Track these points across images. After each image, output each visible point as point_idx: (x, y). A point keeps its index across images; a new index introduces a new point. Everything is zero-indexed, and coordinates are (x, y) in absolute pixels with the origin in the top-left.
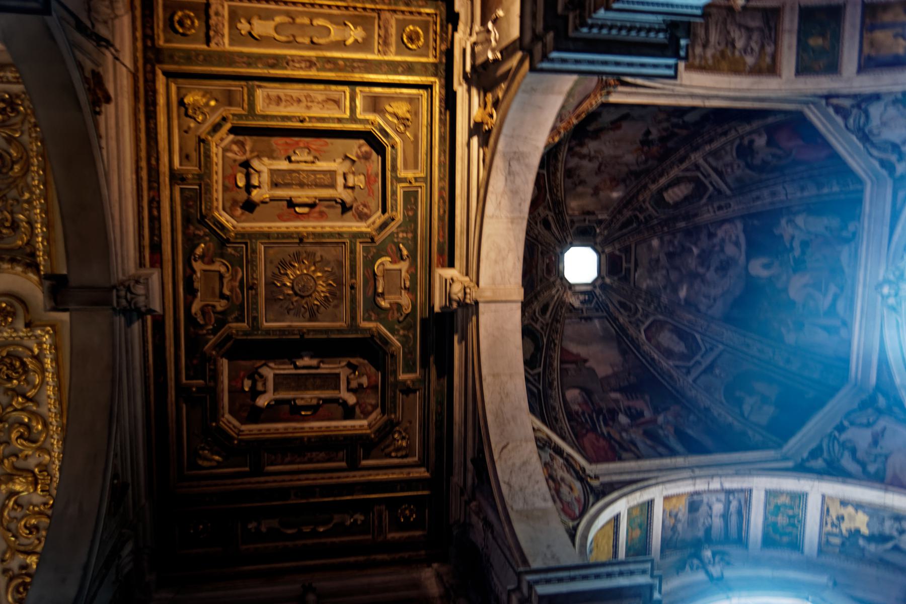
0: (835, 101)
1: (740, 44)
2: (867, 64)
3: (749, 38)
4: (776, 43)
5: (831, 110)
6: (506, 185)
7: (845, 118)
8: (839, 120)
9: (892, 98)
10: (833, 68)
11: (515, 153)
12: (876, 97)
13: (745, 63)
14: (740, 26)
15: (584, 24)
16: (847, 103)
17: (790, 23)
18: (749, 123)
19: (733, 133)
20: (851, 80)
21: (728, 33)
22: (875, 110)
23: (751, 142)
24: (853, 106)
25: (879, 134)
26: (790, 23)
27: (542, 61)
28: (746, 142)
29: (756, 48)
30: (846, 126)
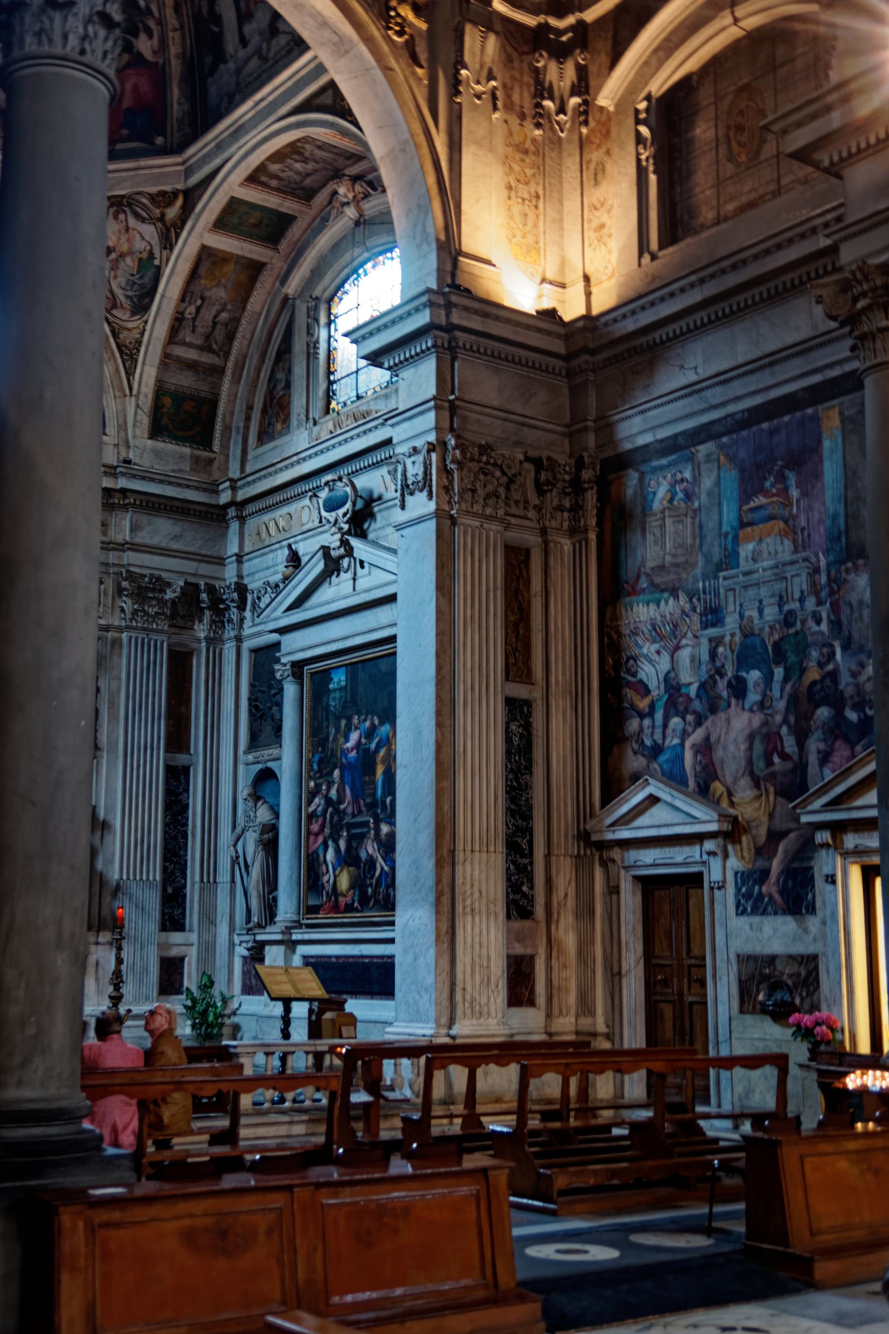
0: (180, 202)
1: (298, 166)
2: (205, 252)
3: (298, 173)
4: (278, 190)
5: (168, 188)
6: (313, 7)
7: (152, 197)
8: (153, 190)
9: (157, 255)
10: (221, 225)
11: (346, 52)
12: (168, 243)
13: (274, 162)
14: (315, 171)
15: (434, 346)
16: (172, 212)
17: (288, 206)
18: (183, 55)
19: (172, 21)
20: (198, 234)
21: (316, 162)
22: (150, 232)
23: (149, 33)
24: (163, 215)
25: (116, 218)
26: (288, 206)
27: (429, 301)
28: (152, 24)
29: (282, 175)
30: (139, 193)
